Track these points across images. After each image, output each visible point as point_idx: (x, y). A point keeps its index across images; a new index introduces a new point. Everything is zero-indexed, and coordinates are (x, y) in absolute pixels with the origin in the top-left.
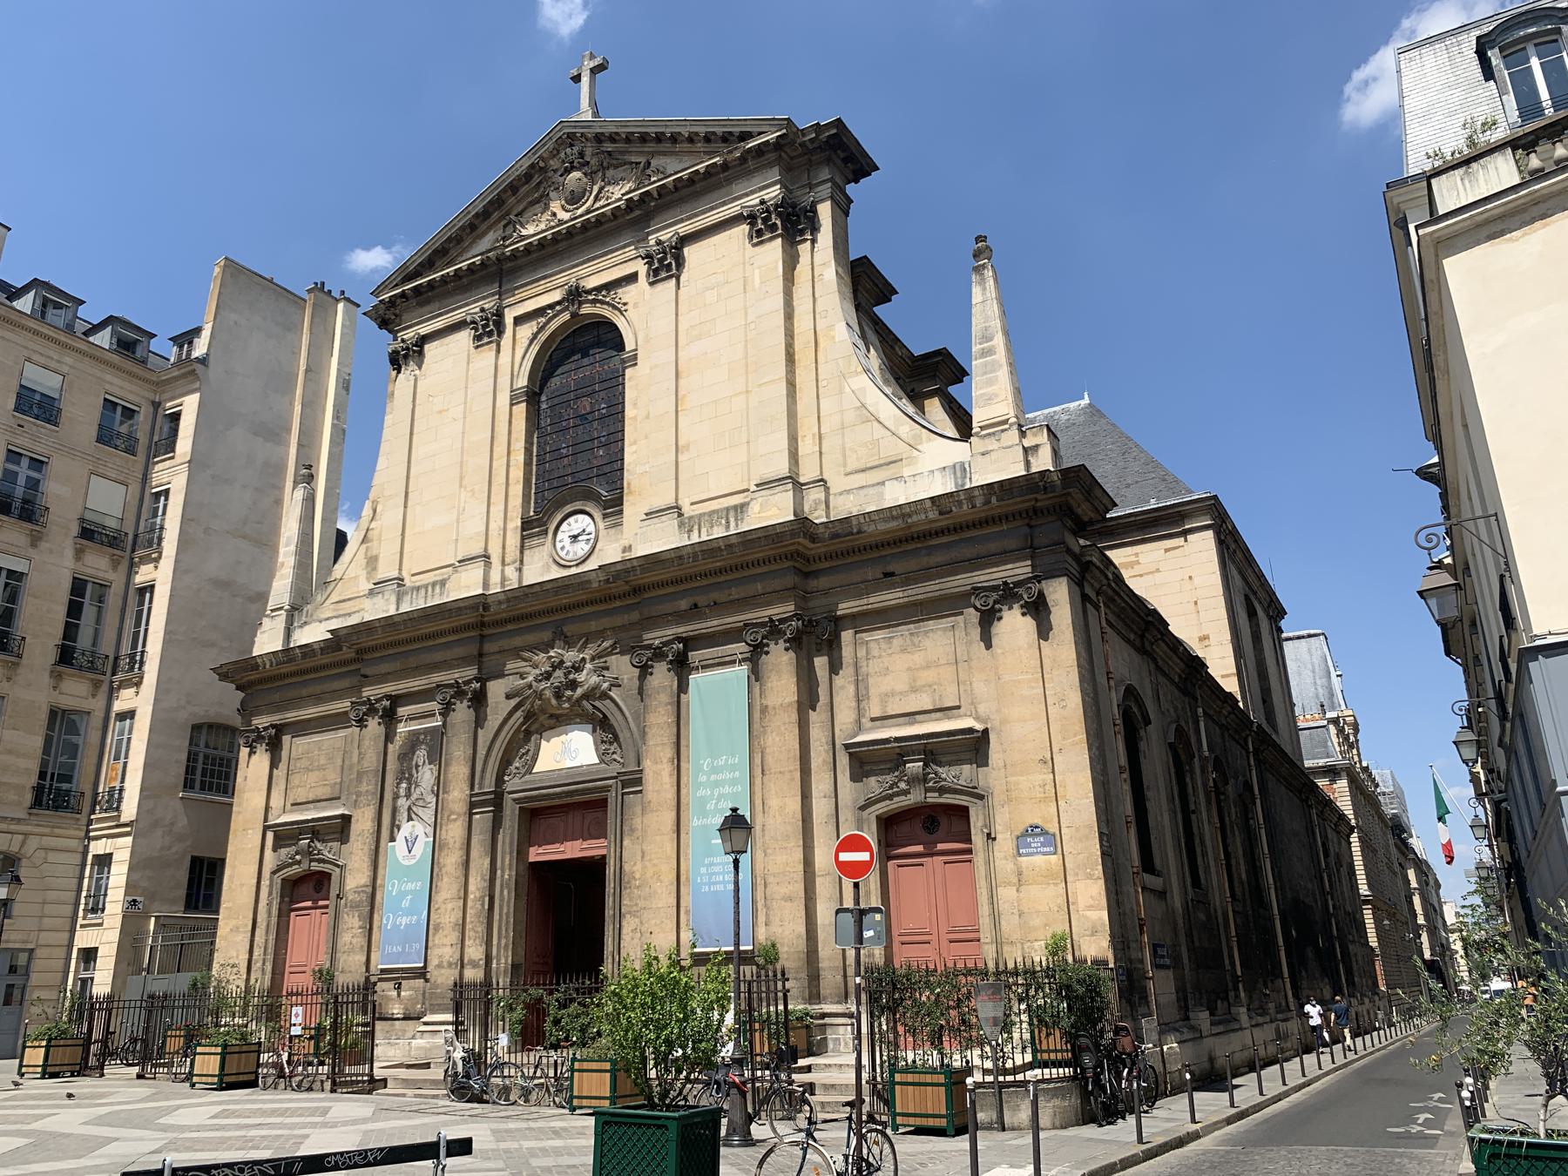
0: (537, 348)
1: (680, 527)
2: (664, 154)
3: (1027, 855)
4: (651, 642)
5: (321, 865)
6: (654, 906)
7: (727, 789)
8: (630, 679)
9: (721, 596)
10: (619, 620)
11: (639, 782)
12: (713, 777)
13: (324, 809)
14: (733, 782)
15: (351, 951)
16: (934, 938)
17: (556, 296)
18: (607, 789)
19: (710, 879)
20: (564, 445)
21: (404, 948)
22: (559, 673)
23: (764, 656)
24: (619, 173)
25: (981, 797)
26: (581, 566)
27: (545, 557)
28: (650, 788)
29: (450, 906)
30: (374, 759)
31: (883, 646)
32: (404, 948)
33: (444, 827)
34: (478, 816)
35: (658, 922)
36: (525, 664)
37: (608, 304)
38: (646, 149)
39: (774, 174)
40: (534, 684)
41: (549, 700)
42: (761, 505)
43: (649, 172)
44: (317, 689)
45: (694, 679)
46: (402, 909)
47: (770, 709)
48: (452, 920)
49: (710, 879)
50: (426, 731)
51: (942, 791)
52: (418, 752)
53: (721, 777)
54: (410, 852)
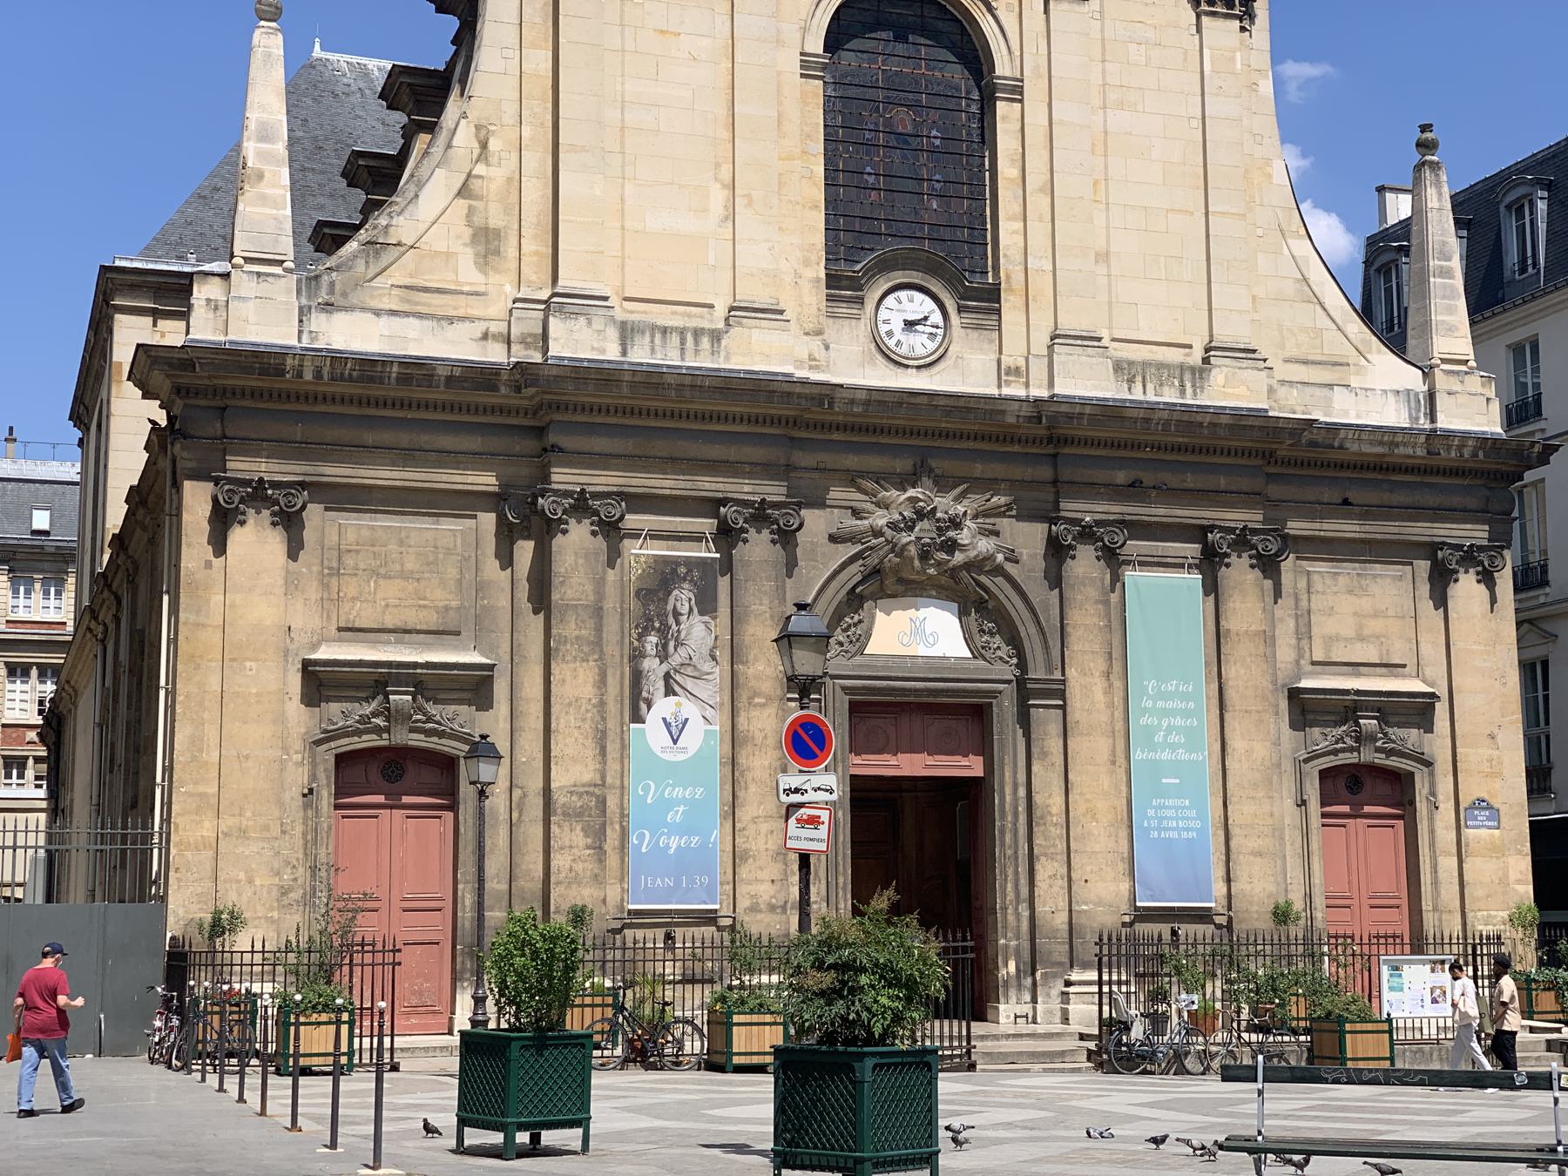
1: (1116, 371)
4: (1079, 516)
5: (435, 739)
6: (1088, 849)
7: (1179, 721)
8: (1033, 556)
9: (1172, 480)
10: (1019, 472)
11: (1062, 694)
12: (1160, 704)
13: (428, 647)
14: (1186, 714)
15: (576, 880)
16: (1355, 902)
18: (994, 694)
19: (1160, 823)
20: (868, 169)
21: (678, 882)
22: (925, 524)
23: (1224, 568)
25: (1429, 764)
26: (925, 372)
27: (862, 339)
28: (1078, 705)
29: (764, 827)
30: (589, 588)
31: (1328, 581)
32: (678, 882)
35: (1095, 869)
41: (912, 559)
42: (1226, 377)
44: (404, 438)
45: (1131, 576)
46: (666, 825)
47: (1233, 635)
48: (769, 846)
49: (1160, 823)
50: (688, 562)
51: (1390, 753)
52: (676, 592)
53: (1170, 705)
54: (675, 742)
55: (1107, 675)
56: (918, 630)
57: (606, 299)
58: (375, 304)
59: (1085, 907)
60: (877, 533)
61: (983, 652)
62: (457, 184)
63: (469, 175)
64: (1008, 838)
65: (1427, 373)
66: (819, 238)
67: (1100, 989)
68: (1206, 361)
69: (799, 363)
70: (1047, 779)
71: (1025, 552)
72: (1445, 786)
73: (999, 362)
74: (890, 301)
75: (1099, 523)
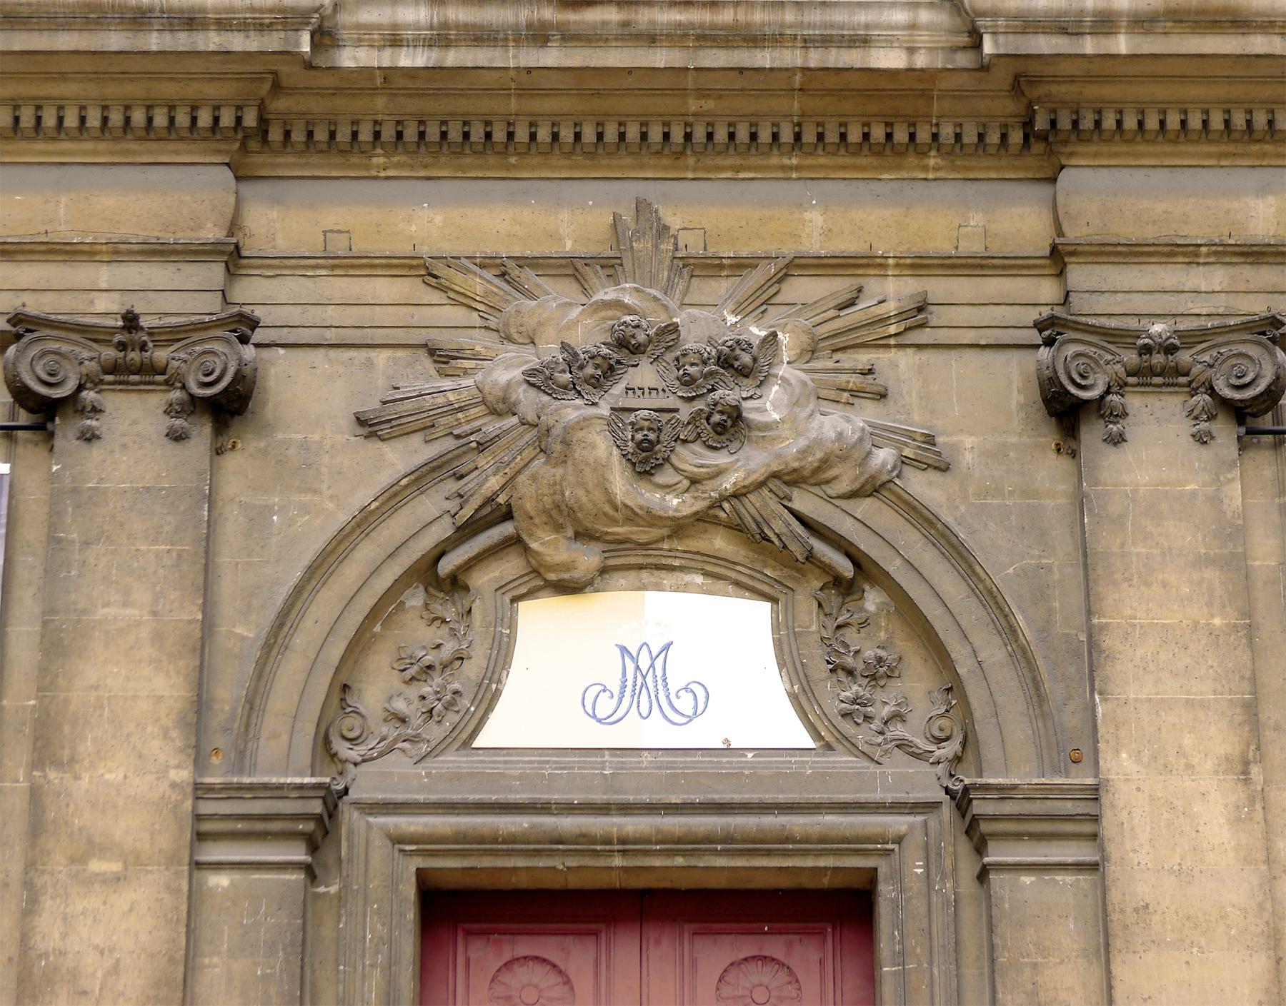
4: (1132, 324)
22: (644, 374)
33: (48, 904)
34: (221, 881)
36: (457, 315)
40: (528, 400)
60: (501, 407)
61: (847, 727)
71: (968, 441)
75: (1190, 339)
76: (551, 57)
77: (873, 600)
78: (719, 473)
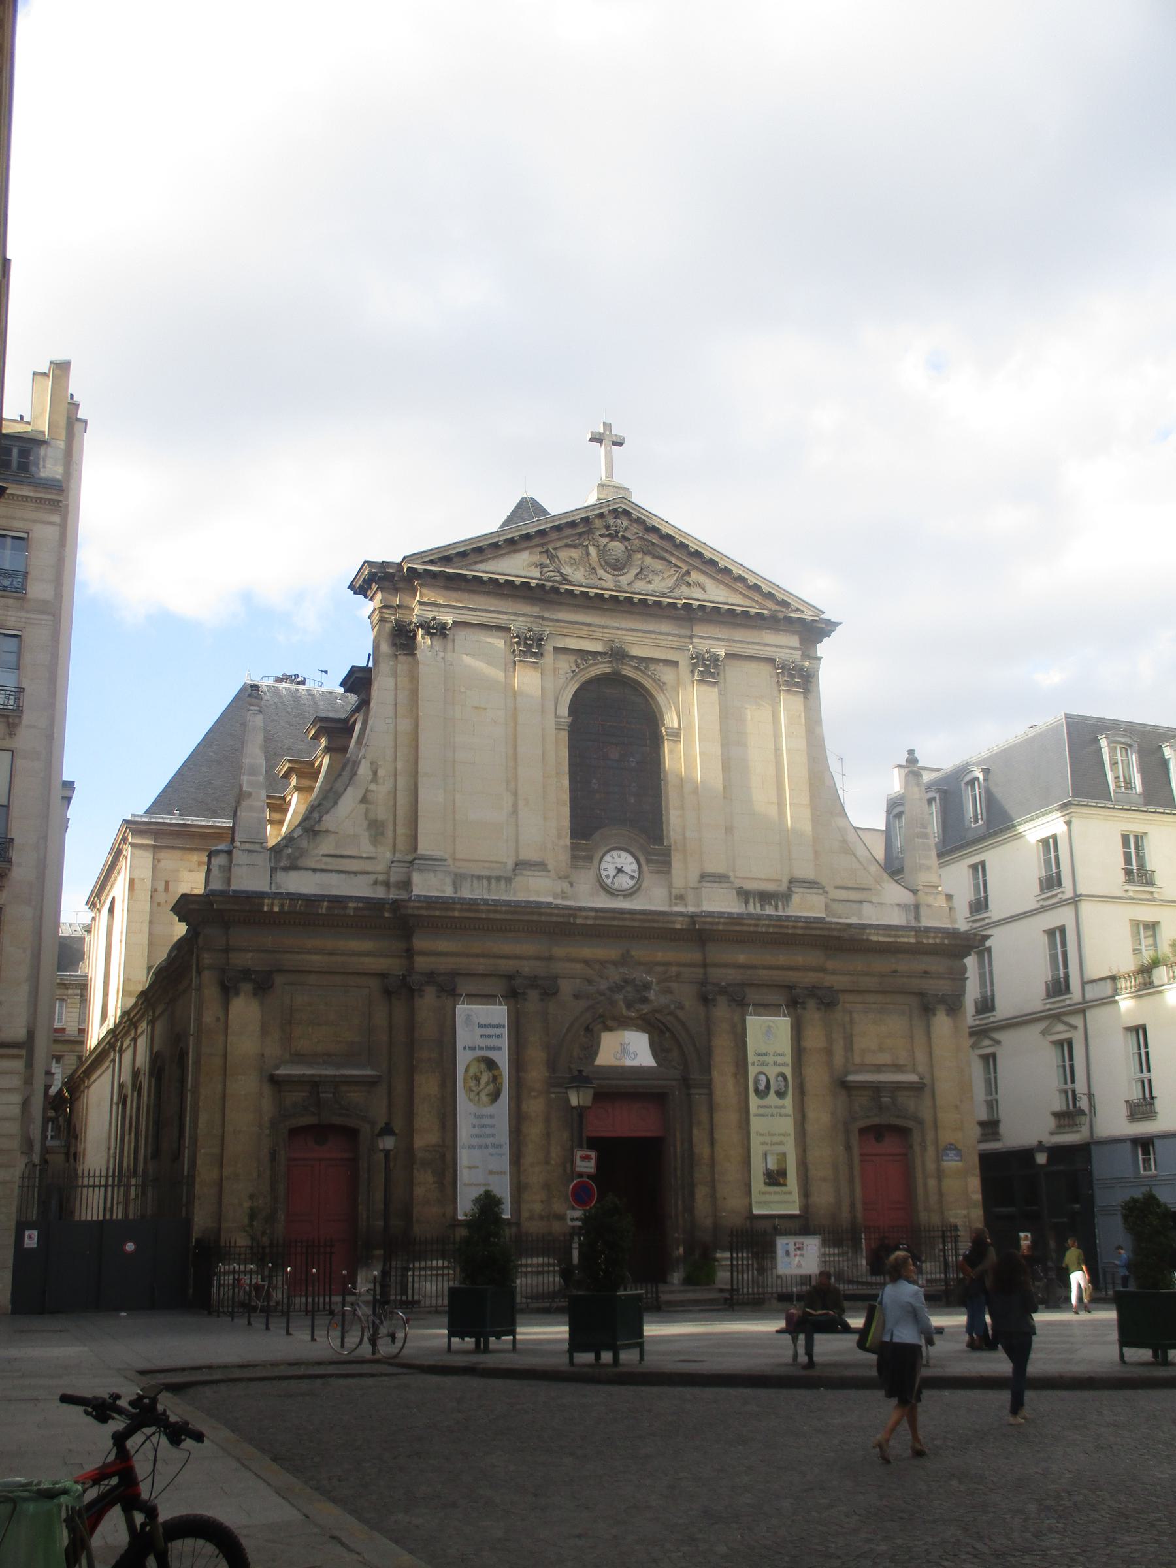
0: (576, 686)
2: (704, 573)
3: (947, 1161)
17: (598, 647)
22: (629, 989)
24: (658, 565)
25: (920, 1122)
34: (553, 1096)
37: (649, 676)
38: (690, 561)
39: (794, 641)
43: (688, 579)
51: (898, 1117)
55: (735, 1075)
56: (624, 1050)
57: (445, 860)
58: (313, 865)
59: (724, 1214)
62: (360, 797)
63: (367, 790)
64: (679, 1173)
65: (914, 892)
66: (566, 822)
67: (732, 1262)
68: (789, 888)
69: (555, 896)
70: (700, 1136)
72: (930, 1136)
73: (670, 893)
74: (608, 858)
76: (615, 923)
77: (668, 1034)
78: (643, 1010)
